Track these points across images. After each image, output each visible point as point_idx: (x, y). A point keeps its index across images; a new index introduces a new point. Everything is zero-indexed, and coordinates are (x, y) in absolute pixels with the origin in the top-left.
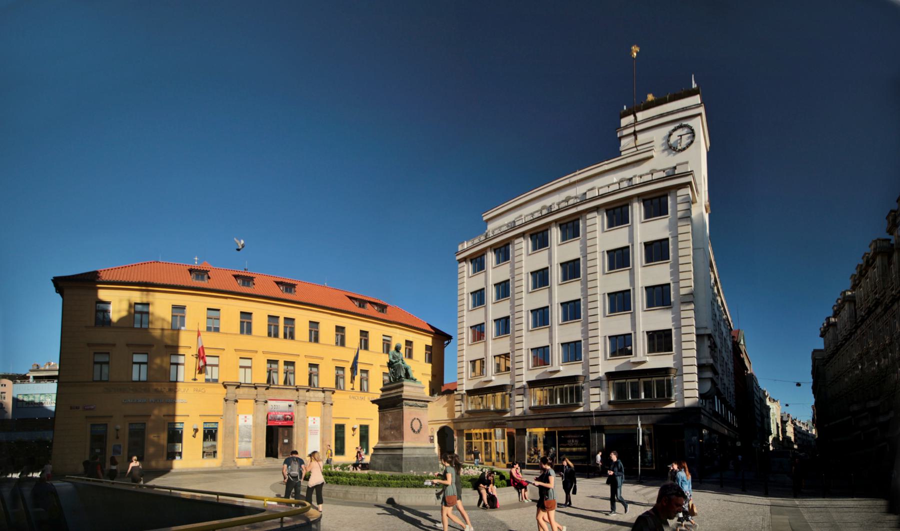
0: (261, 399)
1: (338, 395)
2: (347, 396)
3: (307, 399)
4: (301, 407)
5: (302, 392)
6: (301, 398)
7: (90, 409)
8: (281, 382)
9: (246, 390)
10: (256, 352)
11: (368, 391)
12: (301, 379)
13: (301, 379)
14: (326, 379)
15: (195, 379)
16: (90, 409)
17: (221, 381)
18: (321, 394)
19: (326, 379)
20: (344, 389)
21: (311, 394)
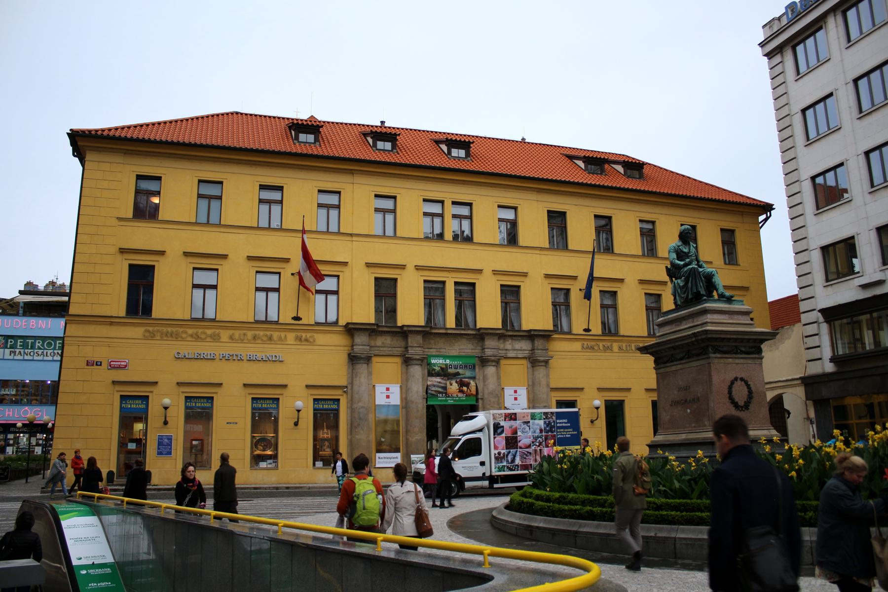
0: (415, 351)
1: (559, 346)
2: (577, 346)
3: (502, 353)
4: (491, 370)
5: (490, 343)
6: (488, 352)
7: (119, 367)
8: (451, 322)
9: (387, 340)
10: (403, 267)
11: (617, 334)
12: (488, 314)
13: (488, 314)
14: (536, 313)
15: (297, 318)
16: (119, 367)
17: (342, 322)
18: (524, 346)
19: (536, 313)
20: (570, 333)
21: (508, 344)
